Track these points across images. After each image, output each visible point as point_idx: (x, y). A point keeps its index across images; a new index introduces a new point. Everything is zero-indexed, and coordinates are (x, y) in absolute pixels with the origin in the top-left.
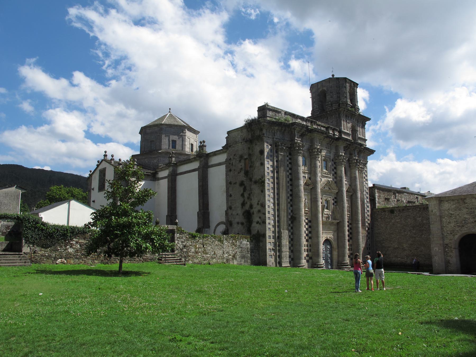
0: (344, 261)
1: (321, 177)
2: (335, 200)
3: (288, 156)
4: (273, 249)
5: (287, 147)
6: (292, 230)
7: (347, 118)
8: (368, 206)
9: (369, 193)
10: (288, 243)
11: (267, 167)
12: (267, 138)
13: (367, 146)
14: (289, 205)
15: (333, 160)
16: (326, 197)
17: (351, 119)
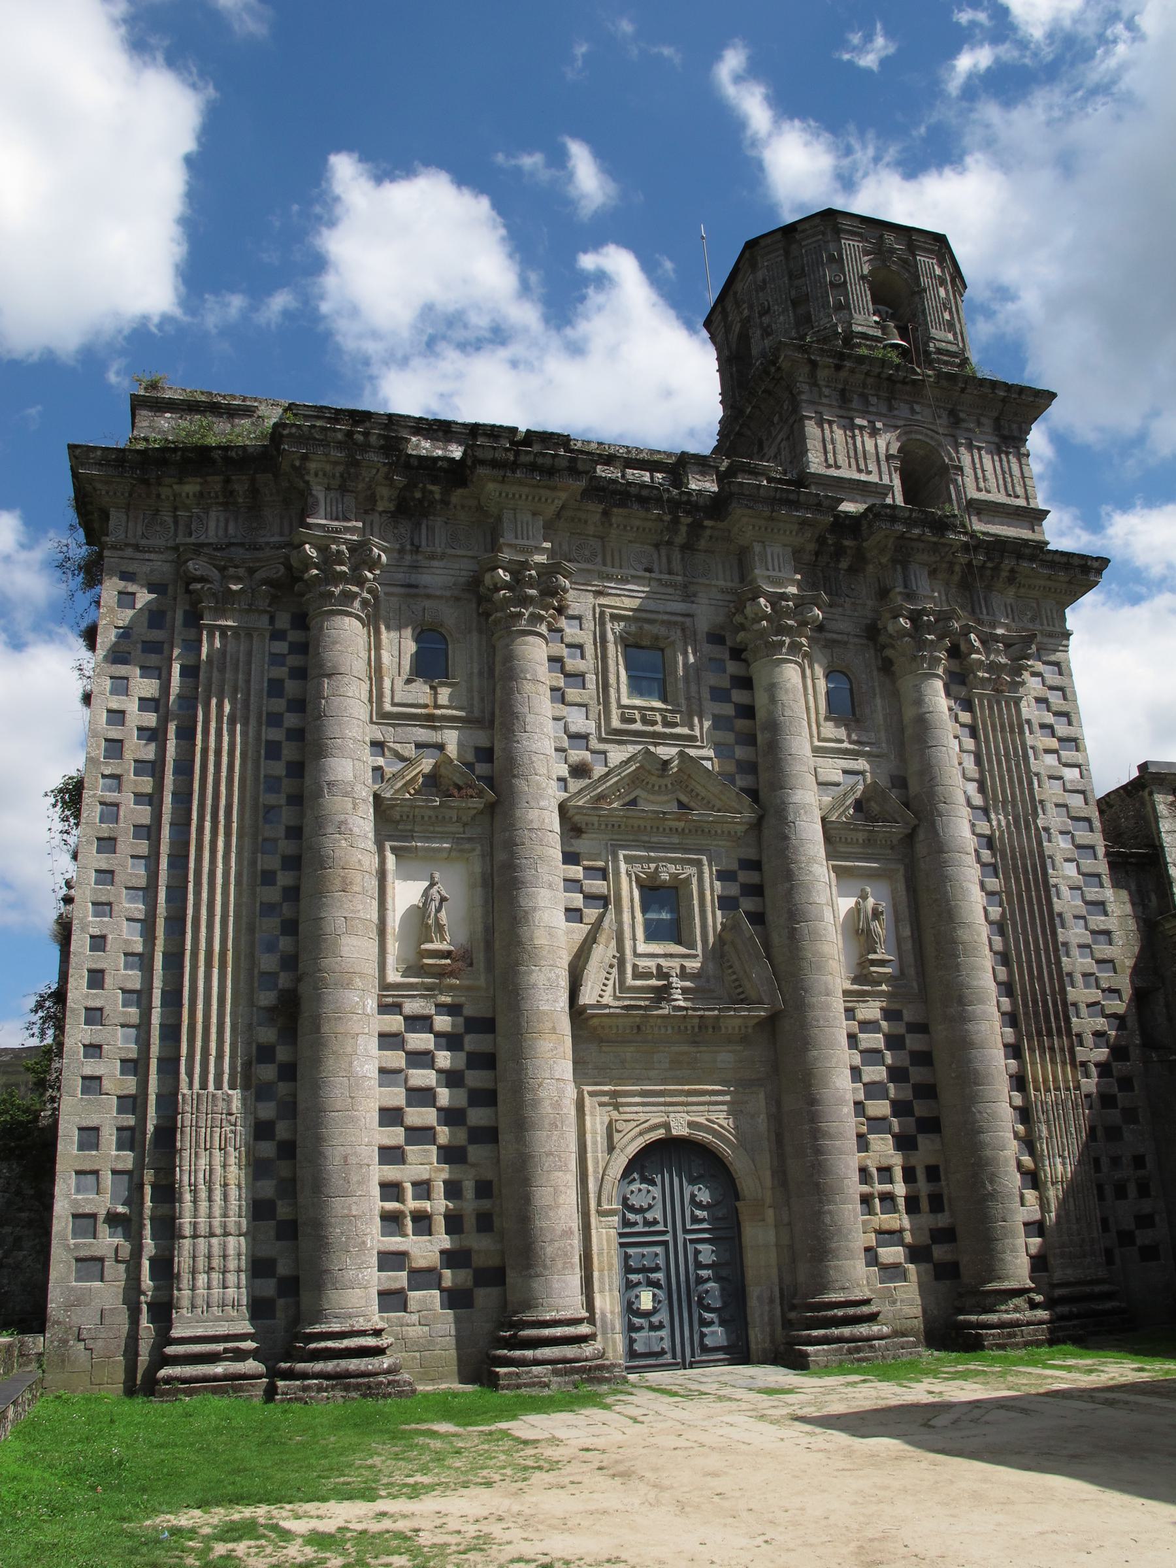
0: (823, 1288)
1: (601, 740)
2: (744, 877)
3: (277, 635)
4: (113, 1219)
5: (266, 582)
6: (283, 1088)
7: (855, 404)
8: (1100, 906)
9: (1097, 824)
10: (235, 1173)
11: (109, 711)
12: (129, 552)
13: (1050, 547)
14: (271, 924)
15: (716, 638)
16: (650, 860)
17: (891, 408)
